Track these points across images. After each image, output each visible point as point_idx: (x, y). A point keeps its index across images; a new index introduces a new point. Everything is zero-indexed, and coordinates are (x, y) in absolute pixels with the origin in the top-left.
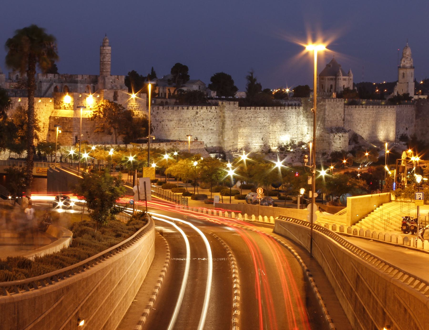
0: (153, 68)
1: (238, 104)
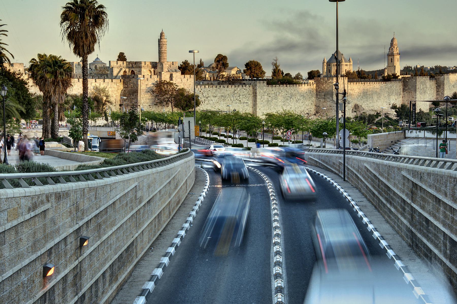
1: (266, 83)
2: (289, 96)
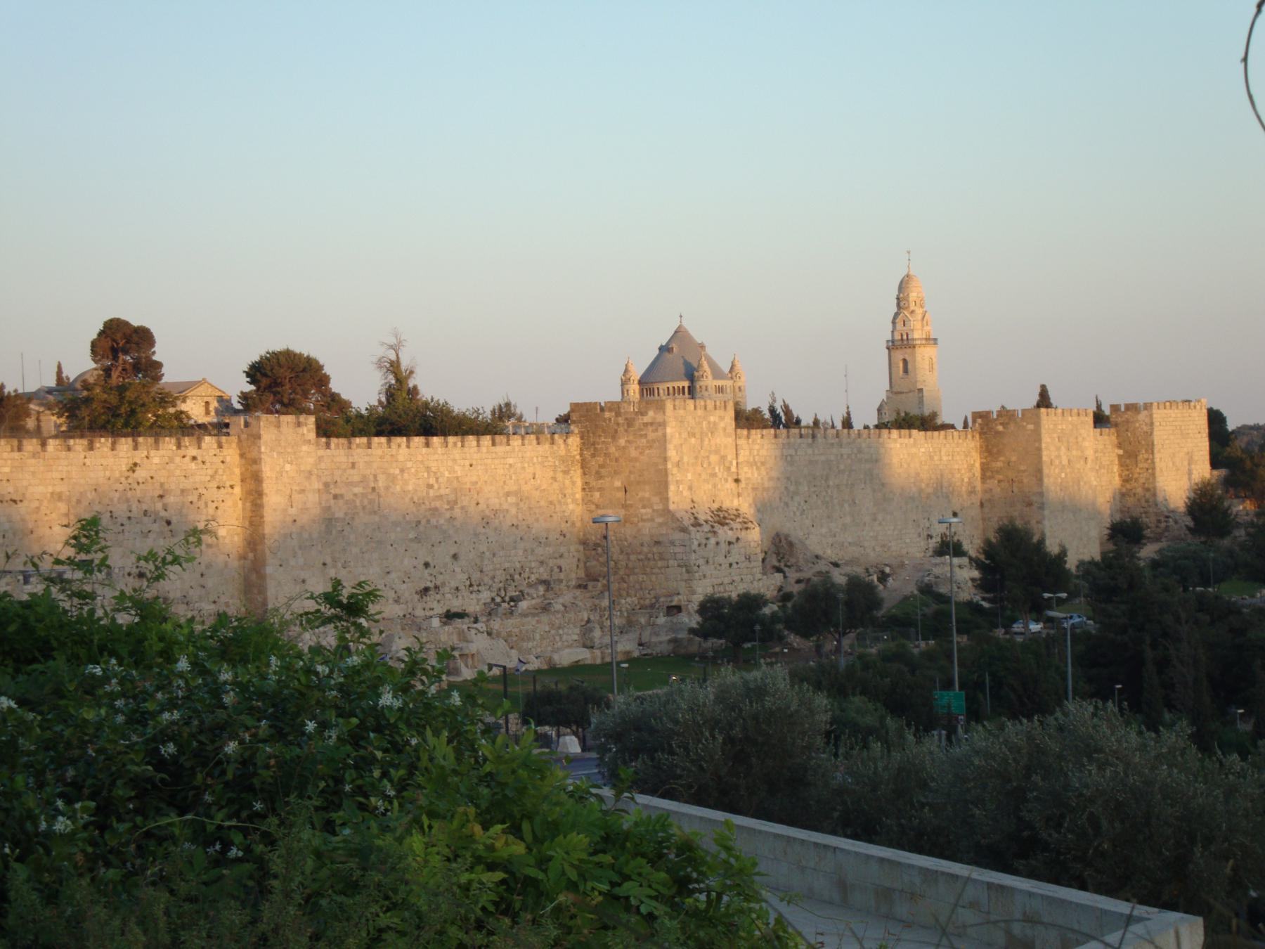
0: (59, 367)
2: (443, 492)
